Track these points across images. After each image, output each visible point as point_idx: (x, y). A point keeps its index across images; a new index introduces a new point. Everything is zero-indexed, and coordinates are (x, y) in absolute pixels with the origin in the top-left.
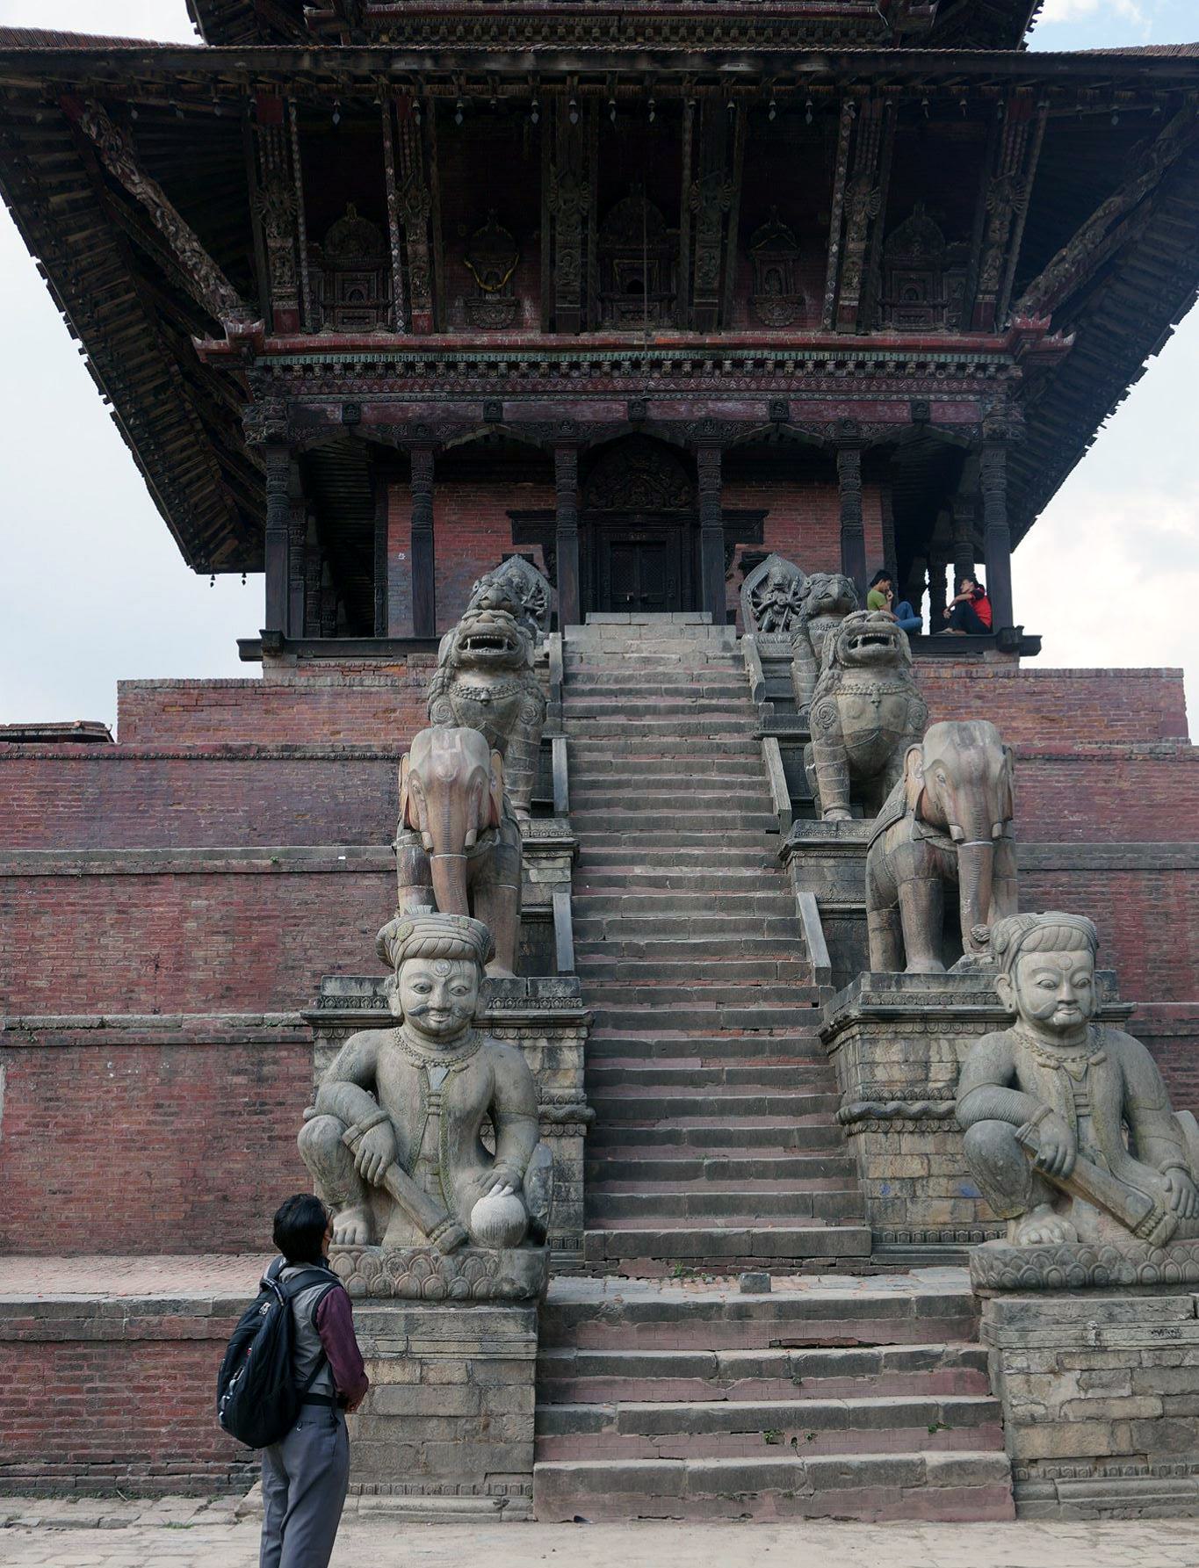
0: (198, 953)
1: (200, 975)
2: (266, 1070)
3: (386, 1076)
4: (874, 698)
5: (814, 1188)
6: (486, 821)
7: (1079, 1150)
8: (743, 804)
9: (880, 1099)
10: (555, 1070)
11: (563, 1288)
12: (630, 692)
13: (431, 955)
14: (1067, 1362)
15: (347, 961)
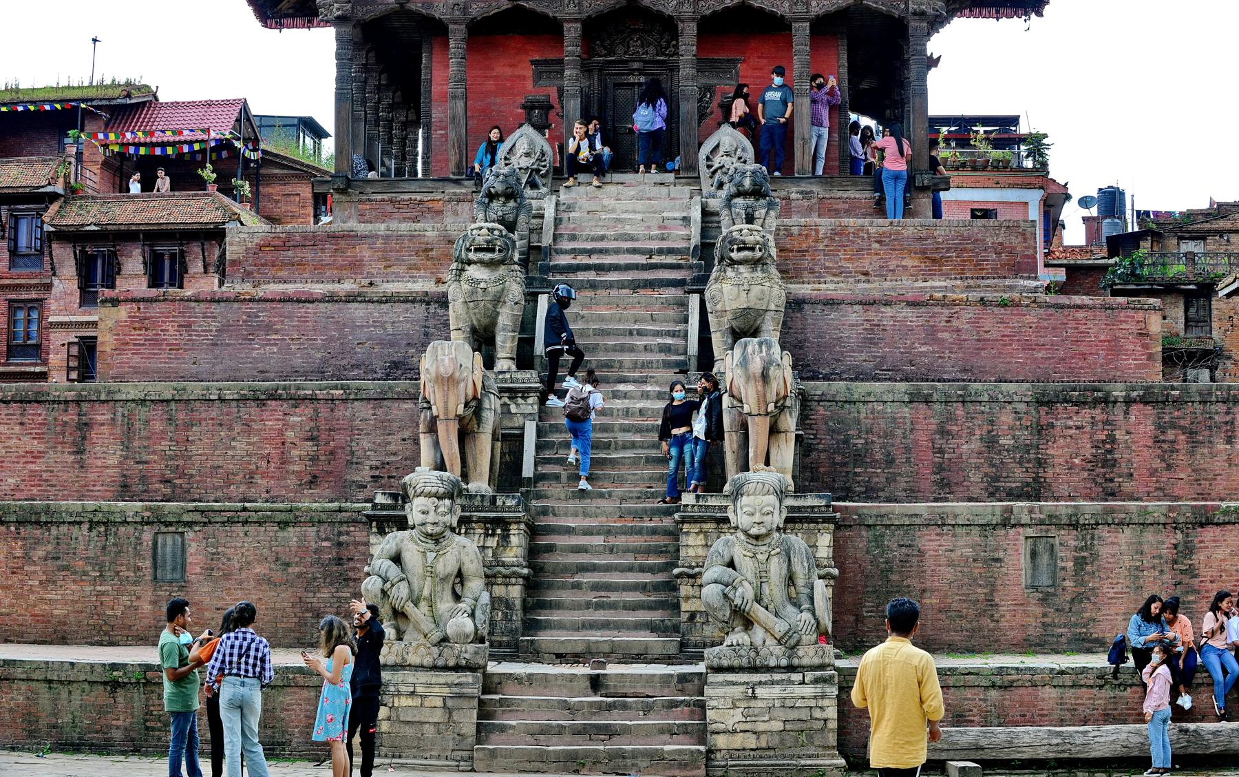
0: (295, 453)
1: (296, 468)
2: (343, 538)
3: (407, 557)
4: (746, 287)
5: (655, 616)
6: (470, 397)
7: (758, 599)
8: (666, 349)
9: (690, 567)
10: (505, 548)
11: (493, 667)
12: (601, 251)
13: (429, 495)
14: (738, 704)
15: (392, 458)
